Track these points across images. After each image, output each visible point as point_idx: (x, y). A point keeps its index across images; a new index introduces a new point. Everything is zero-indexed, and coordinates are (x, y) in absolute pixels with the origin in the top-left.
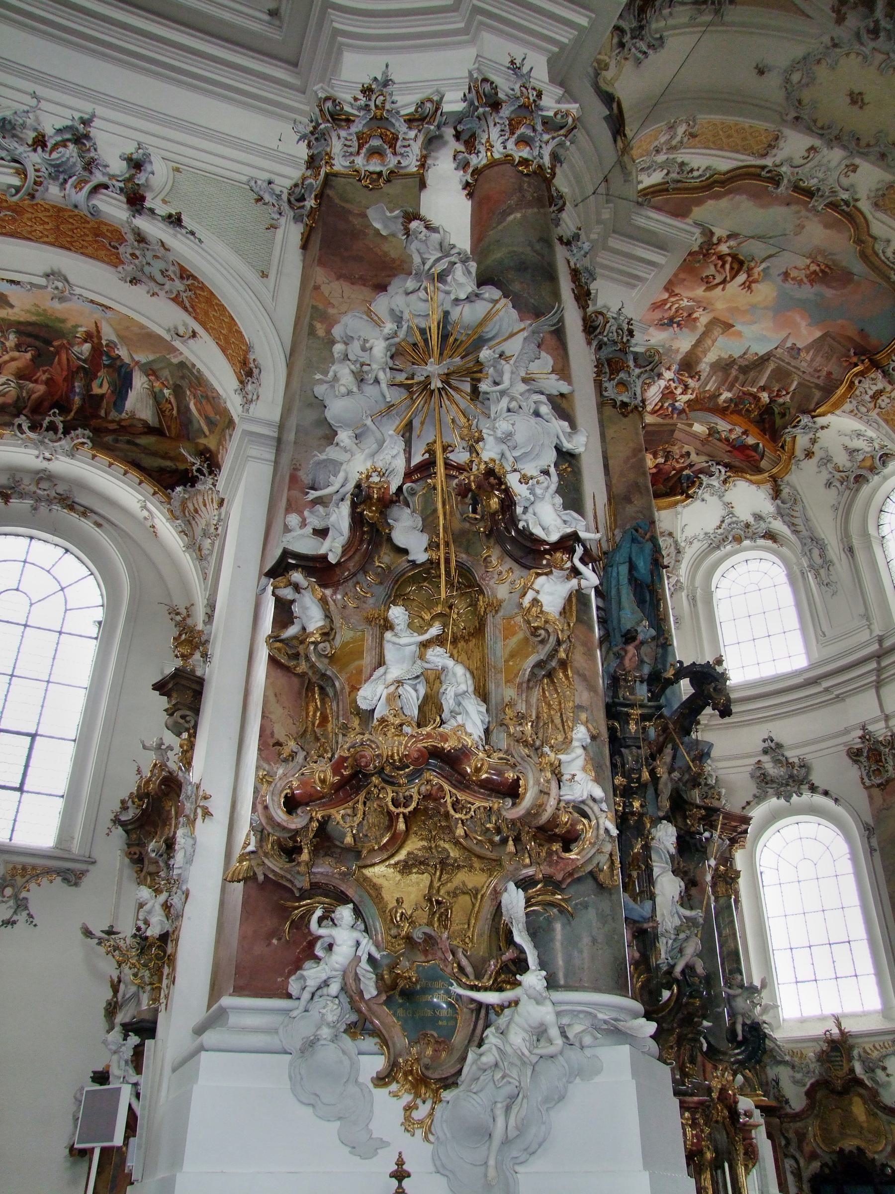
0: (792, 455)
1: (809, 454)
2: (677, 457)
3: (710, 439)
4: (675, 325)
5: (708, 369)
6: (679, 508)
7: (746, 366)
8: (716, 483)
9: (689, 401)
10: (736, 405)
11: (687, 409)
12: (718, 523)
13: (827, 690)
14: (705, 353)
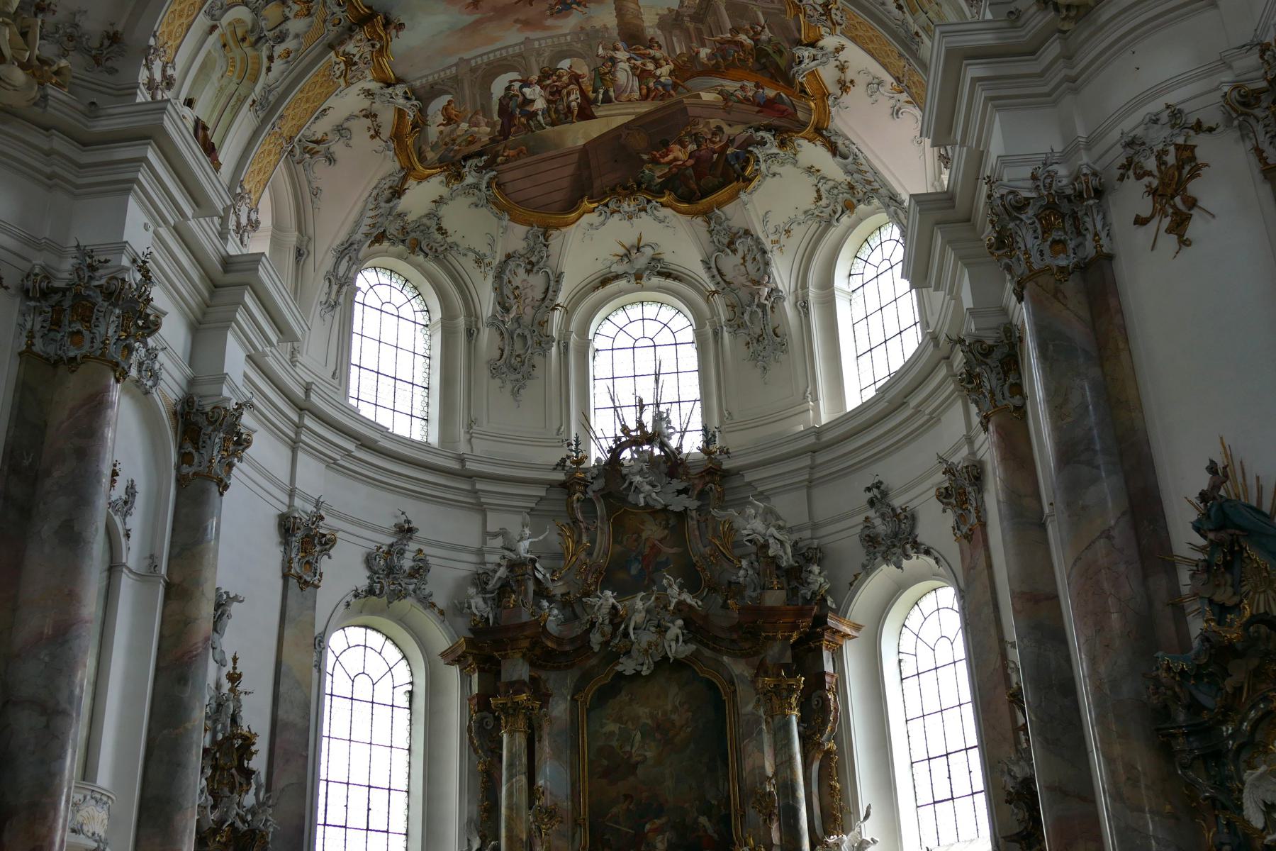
0: (825, 95)
1: (844, 86)
2: (709, 136)
3: (730, 104)
4: (574, 6)
5: (659, 32)
6: (743, 196)
7: (694, 13)
8: (775, 150)
9: (671, 73)
10: (724, 58)
11: (678, 81)
12: (816, 195)
13: (918, 410)
14: (638, 16)
